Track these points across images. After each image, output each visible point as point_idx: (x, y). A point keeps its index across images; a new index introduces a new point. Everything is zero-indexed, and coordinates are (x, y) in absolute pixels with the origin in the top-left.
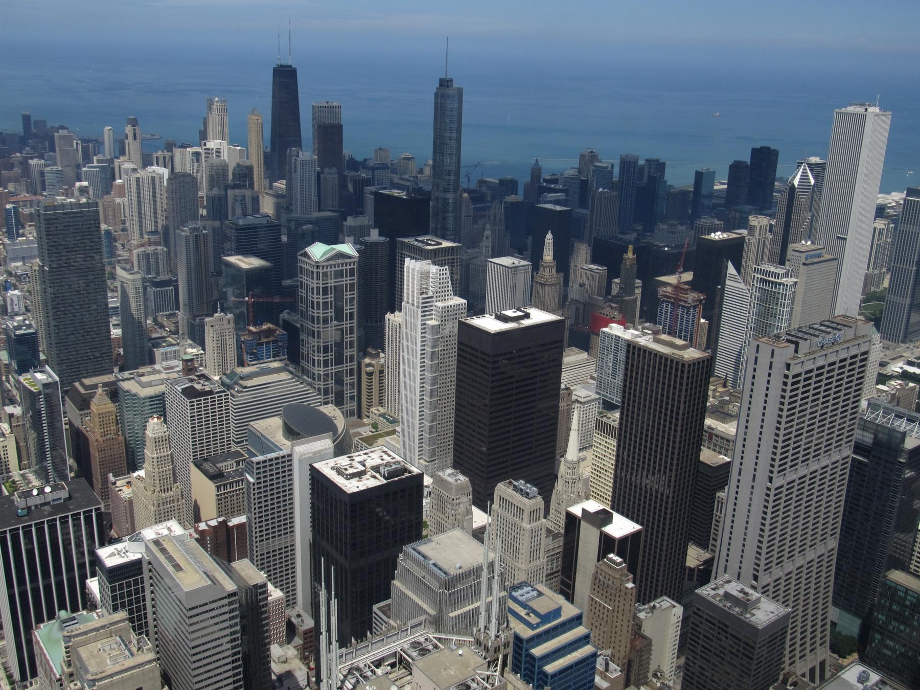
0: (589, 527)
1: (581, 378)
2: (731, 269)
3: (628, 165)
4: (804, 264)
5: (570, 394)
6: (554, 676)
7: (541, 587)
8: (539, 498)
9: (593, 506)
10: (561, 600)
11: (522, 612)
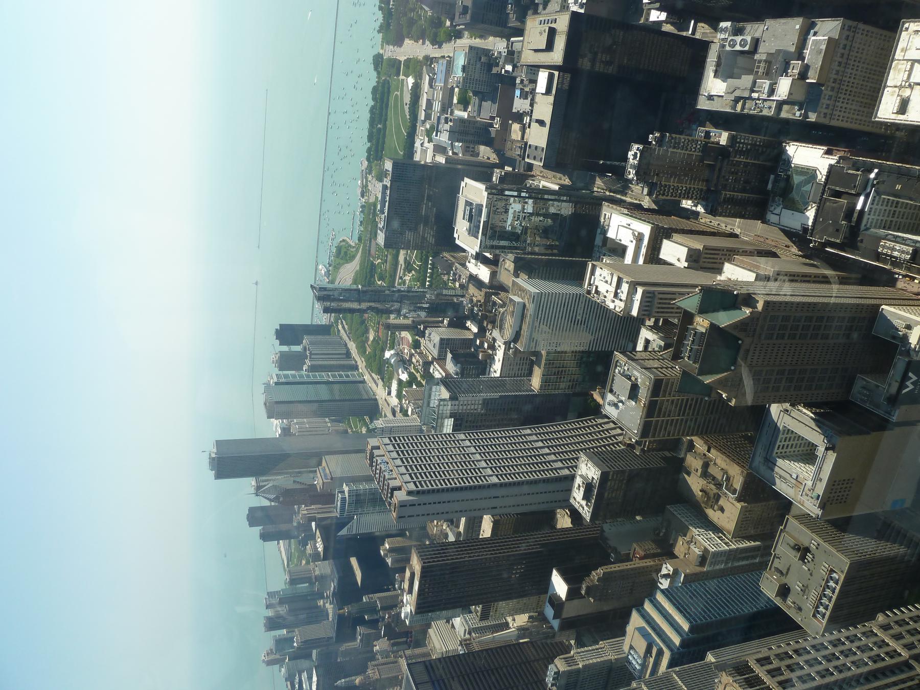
0: (565, 610)
1: (450, 635)
2: (344, 532)
3: (272, 624)
4: (332, 479)
5: (466, 640)
6: (688, 619)
7: (626, 648)
8: (556, 661)
9: (549, 612)
10: (630, 628)
11: (652, 660)
